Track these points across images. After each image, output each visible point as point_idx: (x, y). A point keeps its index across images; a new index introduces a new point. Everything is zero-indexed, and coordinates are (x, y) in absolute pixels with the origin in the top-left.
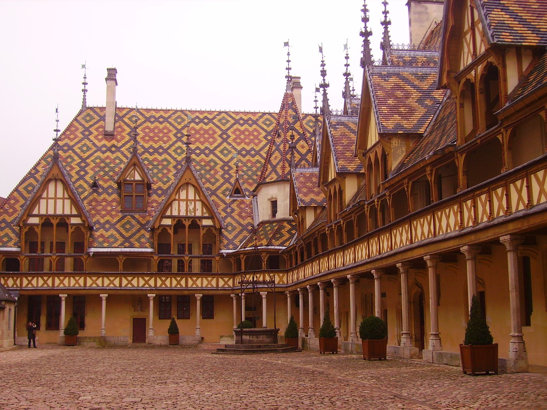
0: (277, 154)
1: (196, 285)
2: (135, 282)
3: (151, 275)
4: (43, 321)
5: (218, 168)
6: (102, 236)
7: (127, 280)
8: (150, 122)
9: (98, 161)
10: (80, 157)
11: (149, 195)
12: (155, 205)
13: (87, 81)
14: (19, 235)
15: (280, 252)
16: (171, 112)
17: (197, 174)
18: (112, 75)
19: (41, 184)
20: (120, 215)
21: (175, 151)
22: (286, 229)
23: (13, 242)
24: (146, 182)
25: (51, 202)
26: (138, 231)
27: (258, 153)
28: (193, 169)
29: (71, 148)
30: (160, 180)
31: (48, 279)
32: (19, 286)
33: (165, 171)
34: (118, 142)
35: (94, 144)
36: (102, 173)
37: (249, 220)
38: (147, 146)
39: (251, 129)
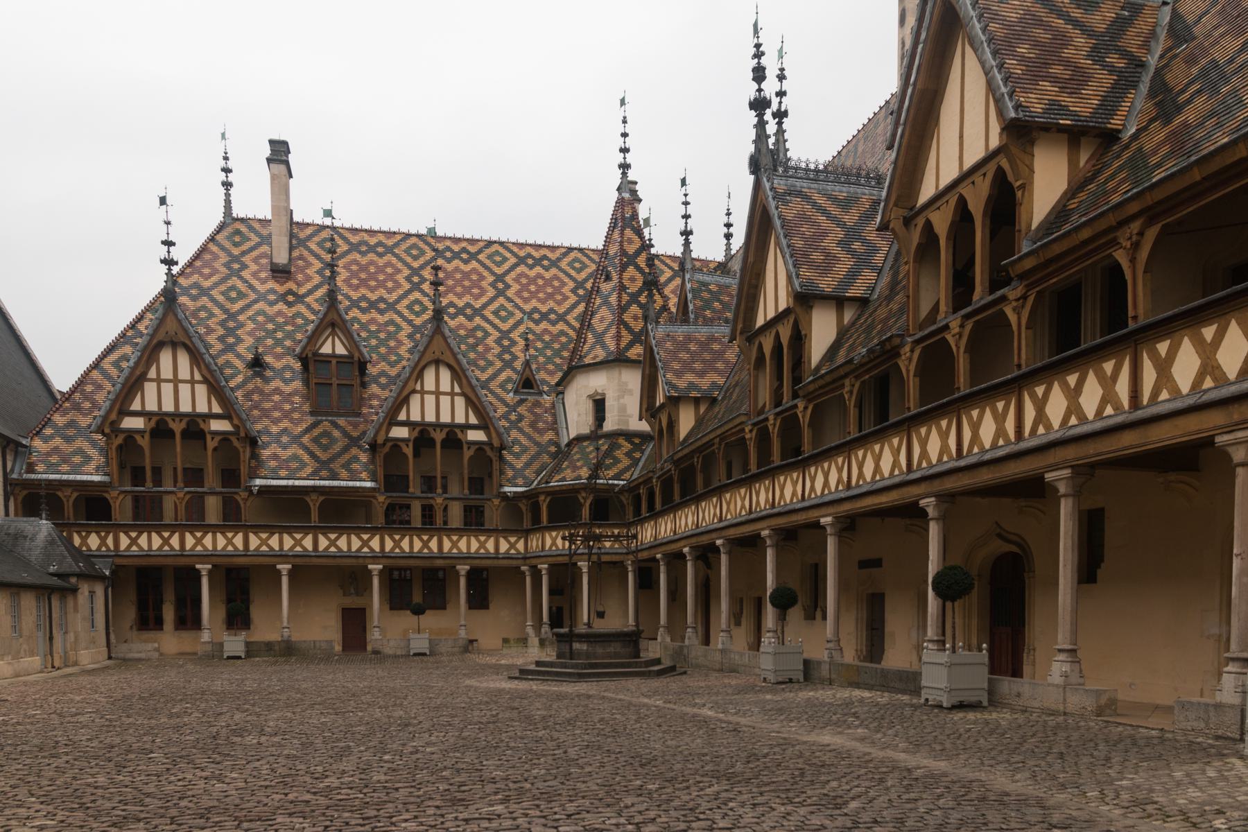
1: (458, 549)
3: (374, 530)
5: (490, 341)
6: (275, 457)
8: (360, 252)
9: (260, 319)
10: (226, 311)
11: (364, 385)
12: (375, 403)
13: (230, 165)
14: (105, 452)
16: (399, 237)
20: (310, 420)
21: (409, 307)
22: (625, 450)
26: (346, 449)
27: (562, 318)
29: (204, 292)
30: (384, 358)
33: (392, 344)
34: (299, 285)
35: (251, 287)
36: (270, 342)
37: (549, 435)
38: (355, 295)
39: (547, 275)
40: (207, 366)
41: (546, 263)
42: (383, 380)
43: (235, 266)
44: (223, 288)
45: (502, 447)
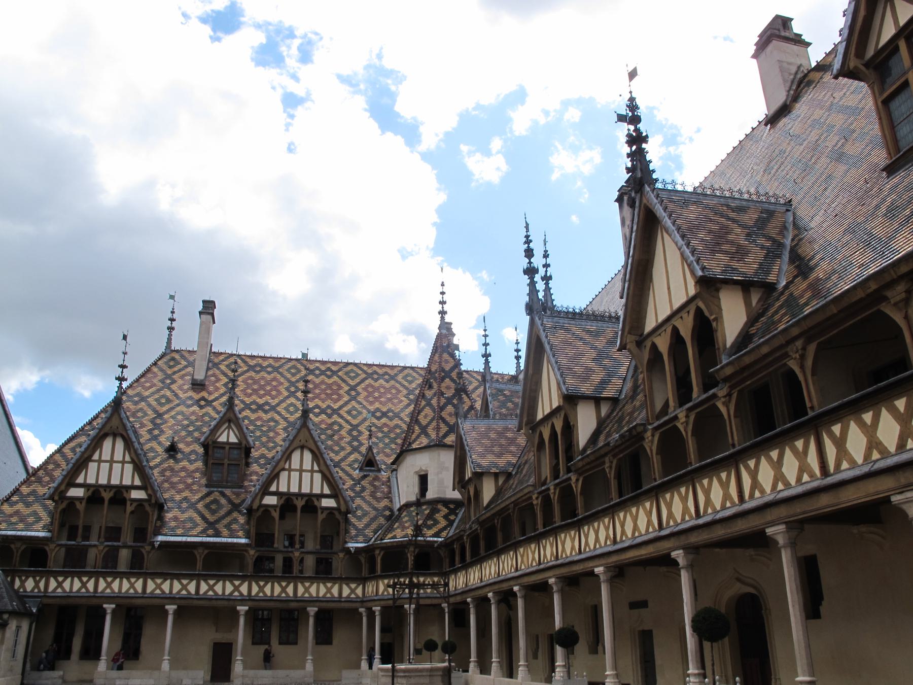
0: (428, 410)
1: (310, 593)
2: (218, 588)
3: (243, 578)
4: (77, 644)
5: (343, 433)
7: (208, 584)
8: (255, 372)
9: (180, 417)
10: (155, 411)
11: (248, 465)
12: (254, 478)
13: (175, 316)
14: (51, 515)
15: (436, 545)
16: (283, 361)
17: (315, 434)
18: (209, 307)
19: (92, 440)
21: (286, 409)
22: (442, 513)
23: (41, 524)
24: (243, 445)
25: (105, 467)
26: (229, 513)
28: (311, 426)
29: (143, 399)
30: (264, 445)
31: (88, 581)
32: (42, 590)
33: (271, 434)
34: (210, 393)
35: (176, 395)
36: (183, 433)
37: (385, 502)
38: (248, 400)
40: (136, 451)
41: (387, 377)
42: (262, 461)
43: (168, 380)
44: (157, 396)
45: (348, 512)
